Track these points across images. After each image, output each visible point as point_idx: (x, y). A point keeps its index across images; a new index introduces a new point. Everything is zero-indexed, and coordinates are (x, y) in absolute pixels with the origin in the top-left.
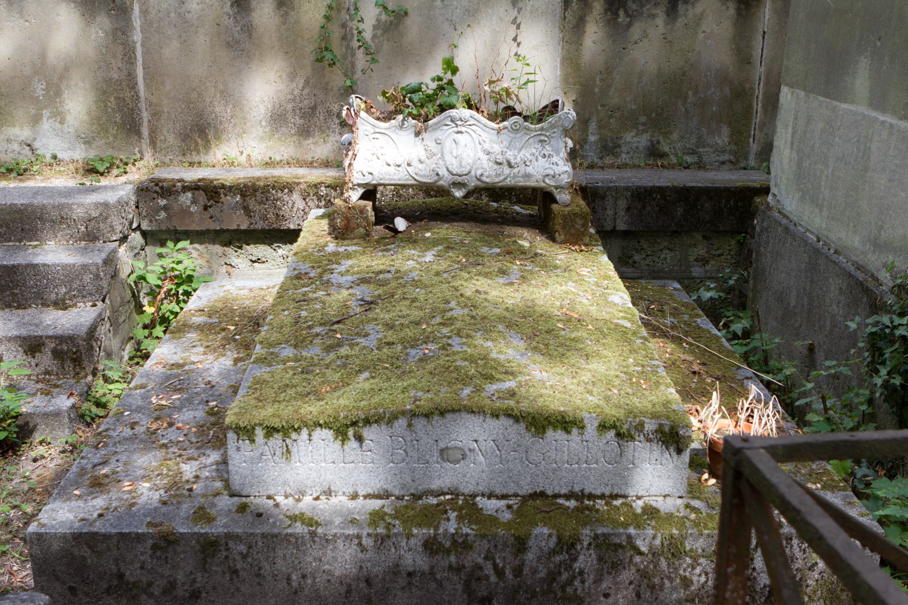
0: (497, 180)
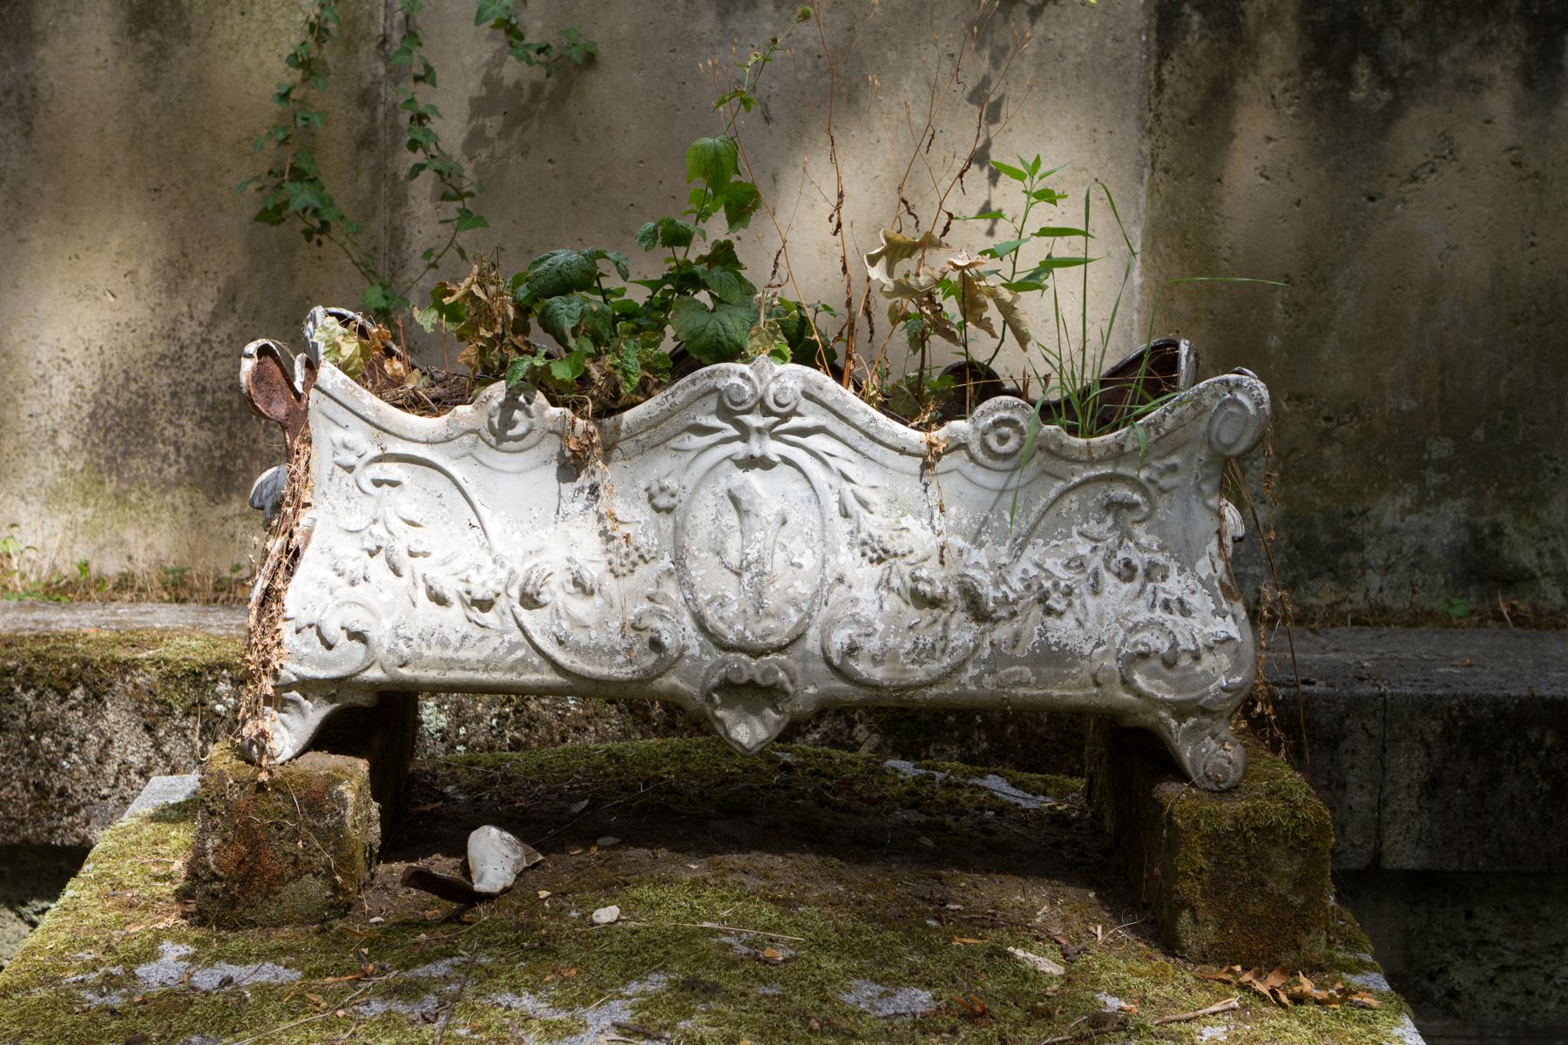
0: (919, 674)
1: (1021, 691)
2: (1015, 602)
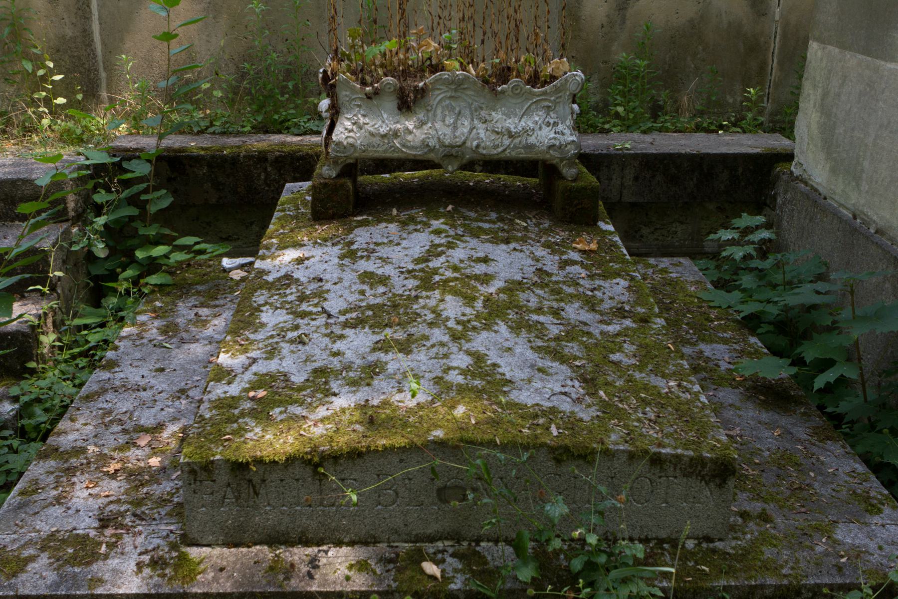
0: (495, 152)
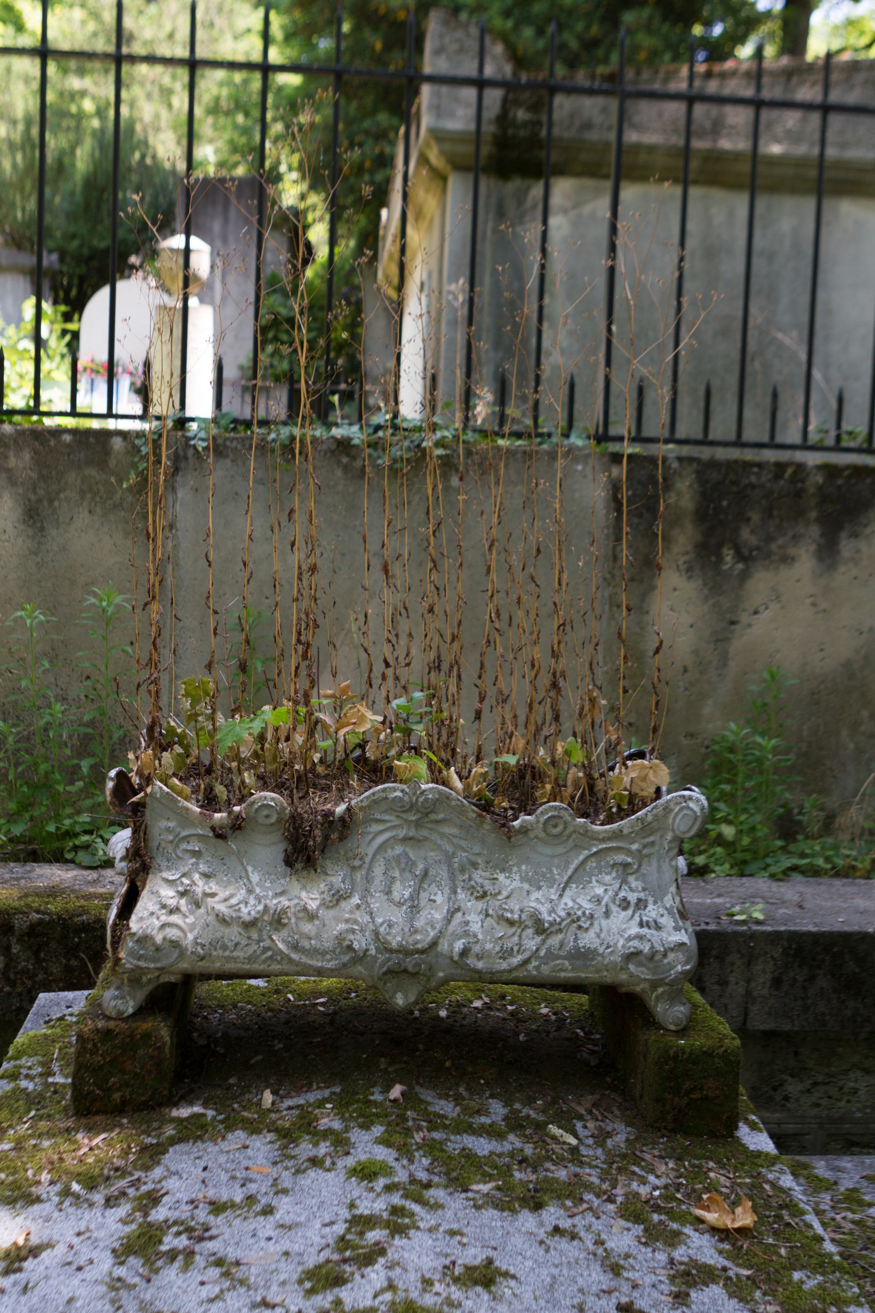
0: (504, 966)
1: (563, 974)
2: (560, 924)
